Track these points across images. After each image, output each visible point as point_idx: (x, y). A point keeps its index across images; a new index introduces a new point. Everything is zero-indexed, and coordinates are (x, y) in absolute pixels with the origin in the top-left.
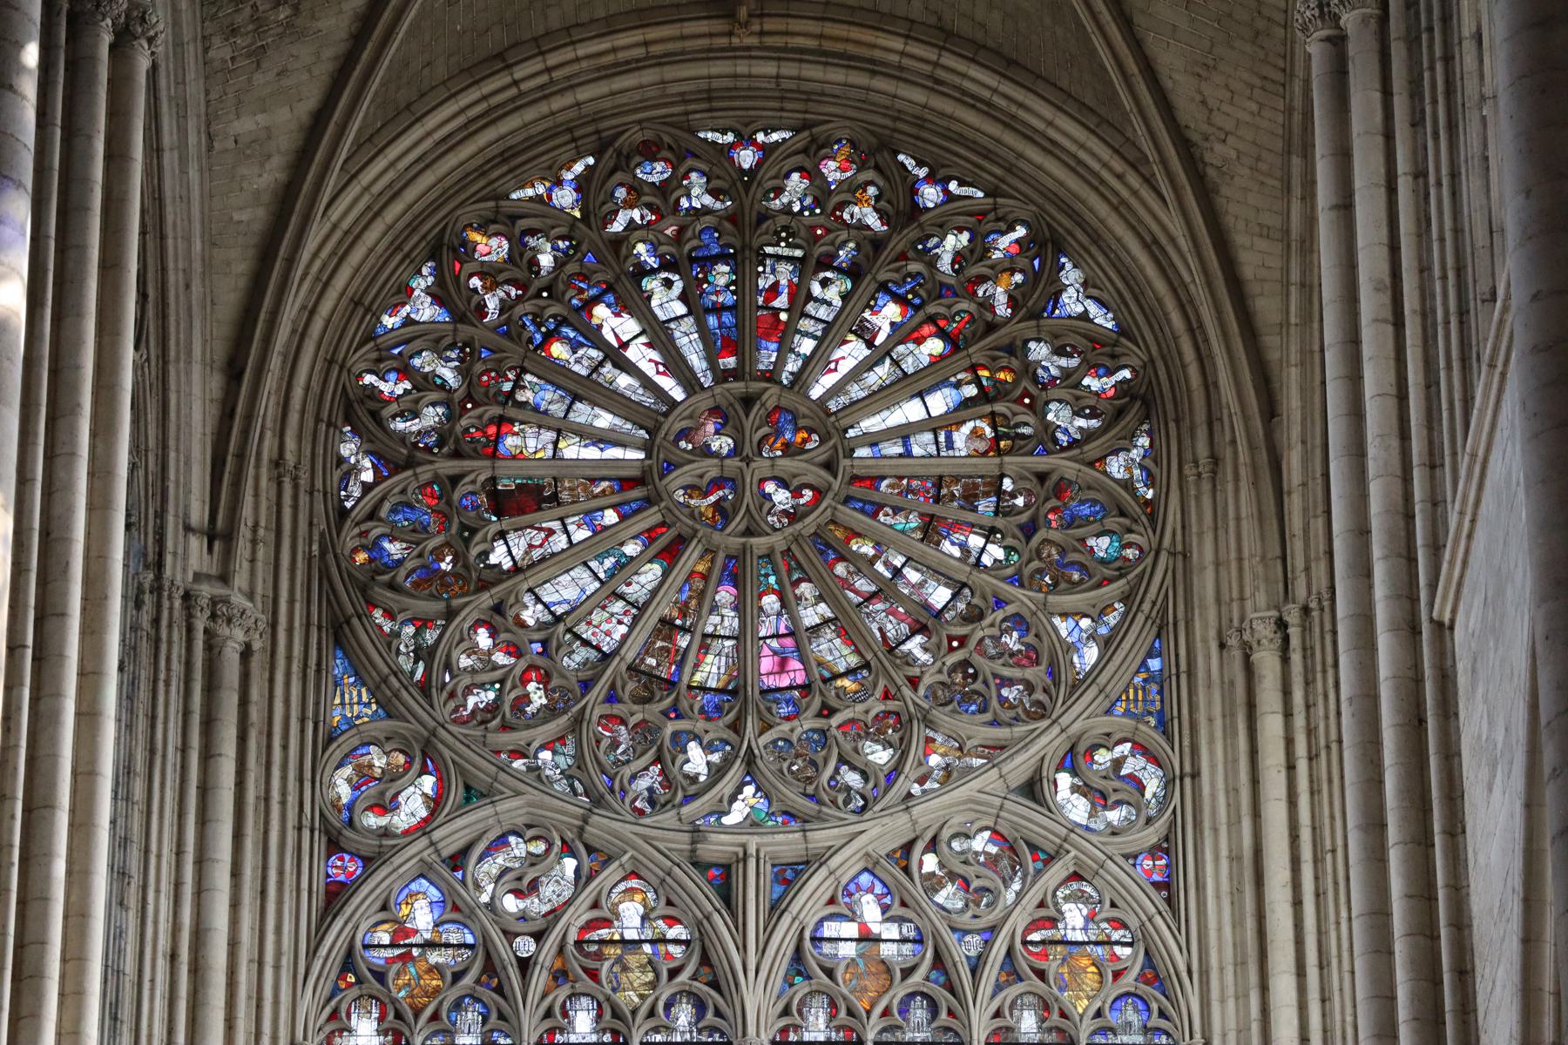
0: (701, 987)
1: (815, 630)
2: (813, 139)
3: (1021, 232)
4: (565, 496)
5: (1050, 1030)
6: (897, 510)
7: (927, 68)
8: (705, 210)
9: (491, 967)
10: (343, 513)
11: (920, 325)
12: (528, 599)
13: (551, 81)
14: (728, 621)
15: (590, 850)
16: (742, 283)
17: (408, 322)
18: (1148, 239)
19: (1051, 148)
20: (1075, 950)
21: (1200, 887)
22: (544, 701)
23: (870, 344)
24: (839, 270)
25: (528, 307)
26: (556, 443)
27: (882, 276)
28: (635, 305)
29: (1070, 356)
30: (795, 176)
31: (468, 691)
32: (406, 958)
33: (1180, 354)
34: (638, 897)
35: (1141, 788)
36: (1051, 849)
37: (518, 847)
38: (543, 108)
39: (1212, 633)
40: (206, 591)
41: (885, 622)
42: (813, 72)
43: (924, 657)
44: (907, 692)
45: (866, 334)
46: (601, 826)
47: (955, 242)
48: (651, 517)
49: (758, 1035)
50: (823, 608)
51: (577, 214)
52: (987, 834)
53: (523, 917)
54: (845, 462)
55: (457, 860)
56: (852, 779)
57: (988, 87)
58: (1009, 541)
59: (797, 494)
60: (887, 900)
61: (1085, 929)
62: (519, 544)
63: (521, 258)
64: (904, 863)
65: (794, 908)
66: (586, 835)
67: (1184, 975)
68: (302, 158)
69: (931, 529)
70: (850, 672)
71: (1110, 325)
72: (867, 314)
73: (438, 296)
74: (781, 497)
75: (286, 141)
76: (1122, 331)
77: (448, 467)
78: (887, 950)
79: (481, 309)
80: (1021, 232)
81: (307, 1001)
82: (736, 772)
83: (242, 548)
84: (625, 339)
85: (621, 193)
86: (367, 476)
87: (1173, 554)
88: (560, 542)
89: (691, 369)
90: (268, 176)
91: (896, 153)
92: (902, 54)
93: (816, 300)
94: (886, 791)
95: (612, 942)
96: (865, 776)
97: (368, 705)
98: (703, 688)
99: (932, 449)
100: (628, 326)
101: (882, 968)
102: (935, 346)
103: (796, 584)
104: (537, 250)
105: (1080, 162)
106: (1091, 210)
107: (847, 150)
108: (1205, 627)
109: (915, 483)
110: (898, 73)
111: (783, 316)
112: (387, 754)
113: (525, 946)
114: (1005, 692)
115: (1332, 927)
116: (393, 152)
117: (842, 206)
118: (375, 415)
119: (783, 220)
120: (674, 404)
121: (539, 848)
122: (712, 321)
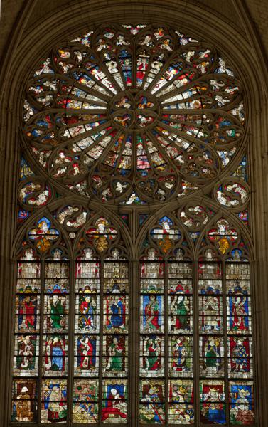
0: (120, 246)
1: (152, 154)
2: (152, 27)
3: (208, 51)
4: (85, 119)
5: (215, 258)
6: (175, 123)
7: (184, 8)
8: (123, 45)
9: (63, 240)
10: (25, 123)
11: (181, 76)
12: (74, 145)
13: (82, 11)
14: (128, 151)
15: (90, 210)
16: (134, 64)
17: (43, 73)
19: (217, 28)
23: (167, 80)
24: (159, 61)
25: (75, 70)
27: (171, 63)
28: (105, 70)
30: (147, 37)
31: (58, 169)
32: (40, 238)
35: (240, 196)
36: (216, 211)
37: (71, 210)
38: (80, 18)
39: (260, 154)
41: (171, 152)
42: (152, 8)
43: (182, 161)
44: (177, 170)
45: (166, 78)
46: (93, 204)
47: (190, 54)
48: (108, 124)
50: (154, 148)
52: (198, 207)
53: (72, 227)
54: (160, 110)
55: (56, 212)
56: (162, 192)
58: (205, 131)
59: (147, 118)
62: (72, 131)
63: (73, 57)
65: (146, 225)
68: (15, 25)
69: (184, 127)
70: (162, 165)
72: (167, 72)
73: (50, 67)
74: (143, 119)
76: (236, 77)
77: (54, 111)
78: (171, 237)
79: (62, 70)
80: (208, 51)
81: (13, 248)
82: (130, 189)
85: (100, 41)
86: (31, 113)
87: (249, 134)
88: (83, 131)
91: (175, 31)
92: (177, 4)
94: (171, 195)
95: (96, 234)
96: (165, 191)
98: (122, 169)
99: (184, 107)
100: (102, 75)
102: (185, 81)
104: (77, 55)
106: (228, 45)
107: (162, 30)
108: (257, 153)
109: (180, 116)
111: (144, 73)
112: (35, 185)
113: (73, 235)
114: (204, 170)
116: (39, 28)
117: (160, 44)
118: (34, 98)
119: (145, 48)
121: (77, 210)
122: (125, 74)
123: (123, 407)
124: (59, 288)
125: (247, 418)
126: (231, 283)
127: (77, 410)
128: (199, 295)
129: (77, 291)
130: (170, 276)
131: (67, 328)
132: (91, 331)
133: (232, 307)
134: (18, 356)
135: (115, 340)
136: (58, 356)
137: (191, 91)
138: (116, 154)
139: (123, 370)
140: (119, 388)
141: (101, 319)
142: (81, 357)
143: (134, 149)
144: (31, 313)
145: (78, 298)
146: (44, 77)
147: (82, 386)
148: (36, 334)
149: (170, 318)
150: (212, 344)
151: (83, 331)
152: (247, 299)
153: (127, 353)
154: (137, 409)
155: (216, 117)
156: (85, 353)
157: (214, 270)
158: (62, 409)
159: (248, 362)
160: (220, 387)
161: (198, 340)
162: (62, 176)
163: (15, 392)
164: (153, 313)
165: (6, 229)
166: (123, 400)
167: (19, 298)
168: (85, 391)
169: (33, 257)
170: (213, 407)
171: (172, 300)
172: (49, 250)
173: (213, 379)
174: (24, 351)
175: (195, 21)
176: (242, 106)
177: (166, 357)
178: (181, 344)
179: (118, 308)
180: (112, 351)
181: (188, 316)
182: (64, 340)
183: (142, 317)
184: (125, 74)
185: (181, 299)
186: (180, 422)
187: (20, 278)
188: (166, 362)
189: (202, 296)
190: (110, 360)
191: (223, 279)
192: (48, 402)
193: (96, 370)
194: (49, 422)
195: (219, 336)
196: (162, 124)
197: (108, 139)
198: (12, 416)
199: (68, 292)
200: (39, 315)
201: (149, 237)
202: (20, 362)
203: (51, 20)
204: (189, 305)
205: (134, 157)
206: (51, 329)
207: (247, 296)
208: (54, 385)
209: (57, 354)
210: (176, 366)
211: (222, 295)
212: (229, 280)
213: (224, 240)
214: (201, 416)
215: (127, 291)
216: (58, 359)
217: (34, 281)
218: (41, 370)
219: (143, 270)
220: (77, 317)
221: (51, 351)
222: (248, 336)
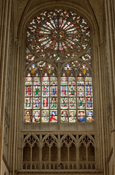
0: (55, 72)
10: (27, 37)
14: (57, 45)
19: (82, 11)
21: (93, 65)
28: (50, 22)
32: (32, 70)
37: (41, 62)
38: (43, 8)
40: (17, 42)
41: (69, 45)
43: (72, 48)
45: (68, 24)
46: (47, 60)
47: (74, 18)
53: (41, 67)
55: (36, 63)
56: (67, 57)
59: (62, 36)
62: (41, 40)
63: (41, 19)
68: (24, 10)
69: (73, 38)
70: (66, 49)
73: (35, 21)
74: (61, 36)
75: (23, 9)
77: (36, 34)
78: (69, 69)
79: (38, 22)
83: (20, 39)
85: (49, 14)
86: (29, 35)
88: (44, 39)
90: (22, 11)
100: (49, 24)
102: (73, 25)
110: (70, 5)
113: (41, 69)
120: (53, 29)
121: (43, 62)
122: (56, 23)
123: (56, 117)
126: (87, 82)
127: (43, 118)
130: (69, 80)
132: (47, 96)
133: (87, 89)
134: (26, 103)
135: (54, 99)
139: (56, 107)
140: (55, 112)
141: (50, 93)
142: (44, 103)
143: (59, 44)
144: (30, 91)
145: (43, 86)
146: (33, 24)
148: (31, 97)
149: (69, 92)
150: (81, 99)
151: (45, 96)
153: (57, 102)
154: (60, 118)
155: (82, 35)
156: (45, 102)
158: (39, 118)
159: (91, 105)
160: (84, 112)
162: (38, 52)
166: (56, 116)
168: (45, 113)
169: (30, 75)
170: (82, 118)
171: (70, 87)
173: (82, 109)
177: (68, 103)
182: (39, 99)
183: (61, 92)
185: (72, 87)
186: (72, 122)
188: (68, 105)
189: (78, 86)
190: (52, 104)
191: (84, 81)
193: (48, 107)
195: (83, 97)
197: (51, 42)
199: (40, 85)
201: (63, 69)
202: (27, 105)
203: (35, 9)
205: (58, 47)
207: (91, 86)
211: (84, 86)
214: (78, 120)
215: (57, 85)
216: (37, 104)
217: (31, 82)
220: (43, 92)
221: (35, 102)
222: (91, 97)
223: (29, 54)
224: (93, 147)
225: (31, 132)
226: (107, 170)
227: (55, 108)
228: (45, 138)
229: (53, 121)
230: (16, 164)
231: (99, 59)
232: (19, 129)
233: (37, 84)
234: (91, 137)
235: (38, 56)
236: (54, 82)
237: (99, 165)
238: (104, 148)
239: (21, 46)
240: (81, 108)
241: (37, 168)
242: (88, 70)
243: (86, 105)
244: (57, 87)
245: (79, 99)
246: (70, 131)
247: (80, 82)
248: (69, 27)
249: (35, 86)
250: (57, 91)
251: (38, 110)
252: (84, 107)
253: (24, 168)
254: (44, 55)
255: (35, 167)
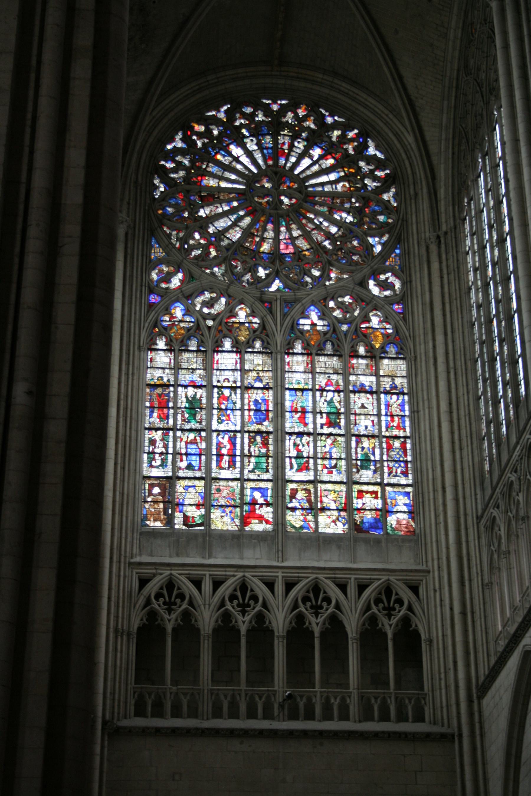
0: (263, 336)
1: (297, 238)
3: (356, 131)
4: (222, 198)
6: (321, 206)
14: (270, 234)
16: (275, 141)
18: (395, 133)
19: (366, 106)
20: (375, 330)
22: (216, 254)
23: (312, 160)
24: (303, 139)
26: (218, 183)
28: (243, 146)
29: (371, 166)
30: (289, 113)
31: (192, 250)
33: (405, 165)
34: (244, 310)
35: (394, 286)
36: (368, 301)
41: (318, 237)
44: (324, 255)
45: (311, 157)
47: (336, 133)
49: (281, 349)
50: (299, 232)
51: (225, 120)
53: (209, 314)
56: (308, 279)
57: (347, 89)
59: (290, 199)
60: (319, 314)
61: (378, 324)
63: (208, 133)
64: (324, 304)
65: (292, 314)
66: (228, 292)
67: (408, 337)
69: (332, 209)
70: (307, 250)
71: (383, 158)
73: (183, 140)
74: (286, 200)
76: (386, 159)
77: (188, 187)
78: (318, 328)
79: (196, 144)
80: (356, 131)
84: (239, 155)
85: (238, 115)
86: (162, 189)
87: (403, 220)
88: (220, 210)
89: (259, 164)
91: (319, 108)
93: (296, 147)
94: (318, 283)
95: (236, 323)
97: (162, 253)
98: (263, 252)
101: (318, 333)
102: (330, 161)
103: (291, 224)
104: (212, 129)
105: (375, 111)
109: (326, 199)
113: (210, 323)
114: (353, 257)
115: (456, 320)
121: (214, 295)
122: (265, 151)
123: (267, 512)
124: (194, 379)
125: (406, 528)
126: (386, 379)
127: (215, 514)
128: (351, 392)
129: (215, 383)
130: (318, 370)
131: (204, 423)
132: (231, 427)
133: (388, 406)
134: (149, 453)
136: (194, 454)
137: (338, 172)
138: (257, 236)
139: (267, 471)
142: (220, 456)
143: (277, 232)
144: (163, 406)
145: (216, 390)
147: (222, 488)
148: (168, 429)
149: (318, 416)
151: (222, 427)
152: (404, 397)
153: (271, 453)
154: (284, 515)
155: (366, 200)
156: (224, 451)
157: (367, 365)
159: (406, 466)
160: (376, 493)
161: (351, 440)
162: (196, 257)
163: (145, 493)
164: (299, 409)
165: (135, 313)
166: (268, 504)
167: (150, 388)
168: (225, 493)
169: (166, 345)
170: (369, 516)
171: (321, 396)
172: (184, 337)
174: (155, 448)
175: (342, 98)
176: (393, 190)
177: (315, 458)
178: (332, 444)
179: (261, 404)
180: (255, 450)
181: (338, 414)
182: (200, 437)
183: (288, 415)
184: (265, 151)
185: (330, 394)
187: (151, 368)
188: (315, 464)
189: (354, 392)
190: (253, 460)
191: (377, 375)
192: (183, 505)
193: (238, 470)
194: (184, 527)
195: (373, 436)
196: (307, 205)
197: (247, 220)
198: (142, 520)
199: (204, 383)
200: (172, 408)
201: (294, 326)
202: (151, 459)
204: (340, 401)
205: (277, 240)
206: (186, 424)
207: (403, 394)
208: (190, 487)
209: (193, 452)
210: (327, 468)
211: (376, 393)
212: (384, 376)
213: (378, 334)
214: (356, 524)
215: (271, 385)
216: (194, 458)
217: (167, 371)
218: (175, 469)
219: (289, 363)
220: (215, 412)
221: (187, 448)
222: (405, 437)
223: (161, 261)
224: (416, 634)
225: (169, 565)
226: (477, 726)
227: (265, 476)
228: (225, 590)
229: (256, 526)
230: (108, 695)
231: (437, 289)
232: (123, 553)
233: (192, 381)
234: (406, 595)
235: (195, 271)
236: (261, 374)
237: (442, 707)
238: (459, 638)
239: (130, 232)
240: (364, 479)
241: (194, 713)
242: (390, 331)
243: (386, 470)
244: (270, 395)
245: (357, 443)
246: (324, 569)
247: (362, 379)
248: (316, 168)
249: (186, 387)
250: (271, 408)
251: (196, 483)
252: (378, 476)
253: (140, 712)
254: (222, 271)
255: (185, 708)
